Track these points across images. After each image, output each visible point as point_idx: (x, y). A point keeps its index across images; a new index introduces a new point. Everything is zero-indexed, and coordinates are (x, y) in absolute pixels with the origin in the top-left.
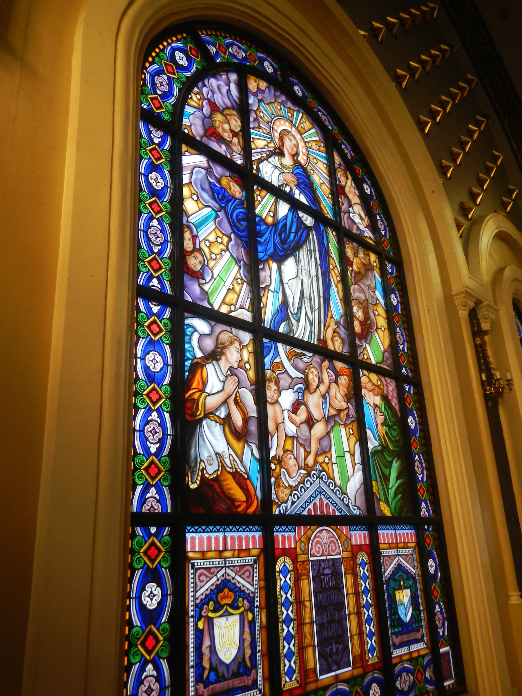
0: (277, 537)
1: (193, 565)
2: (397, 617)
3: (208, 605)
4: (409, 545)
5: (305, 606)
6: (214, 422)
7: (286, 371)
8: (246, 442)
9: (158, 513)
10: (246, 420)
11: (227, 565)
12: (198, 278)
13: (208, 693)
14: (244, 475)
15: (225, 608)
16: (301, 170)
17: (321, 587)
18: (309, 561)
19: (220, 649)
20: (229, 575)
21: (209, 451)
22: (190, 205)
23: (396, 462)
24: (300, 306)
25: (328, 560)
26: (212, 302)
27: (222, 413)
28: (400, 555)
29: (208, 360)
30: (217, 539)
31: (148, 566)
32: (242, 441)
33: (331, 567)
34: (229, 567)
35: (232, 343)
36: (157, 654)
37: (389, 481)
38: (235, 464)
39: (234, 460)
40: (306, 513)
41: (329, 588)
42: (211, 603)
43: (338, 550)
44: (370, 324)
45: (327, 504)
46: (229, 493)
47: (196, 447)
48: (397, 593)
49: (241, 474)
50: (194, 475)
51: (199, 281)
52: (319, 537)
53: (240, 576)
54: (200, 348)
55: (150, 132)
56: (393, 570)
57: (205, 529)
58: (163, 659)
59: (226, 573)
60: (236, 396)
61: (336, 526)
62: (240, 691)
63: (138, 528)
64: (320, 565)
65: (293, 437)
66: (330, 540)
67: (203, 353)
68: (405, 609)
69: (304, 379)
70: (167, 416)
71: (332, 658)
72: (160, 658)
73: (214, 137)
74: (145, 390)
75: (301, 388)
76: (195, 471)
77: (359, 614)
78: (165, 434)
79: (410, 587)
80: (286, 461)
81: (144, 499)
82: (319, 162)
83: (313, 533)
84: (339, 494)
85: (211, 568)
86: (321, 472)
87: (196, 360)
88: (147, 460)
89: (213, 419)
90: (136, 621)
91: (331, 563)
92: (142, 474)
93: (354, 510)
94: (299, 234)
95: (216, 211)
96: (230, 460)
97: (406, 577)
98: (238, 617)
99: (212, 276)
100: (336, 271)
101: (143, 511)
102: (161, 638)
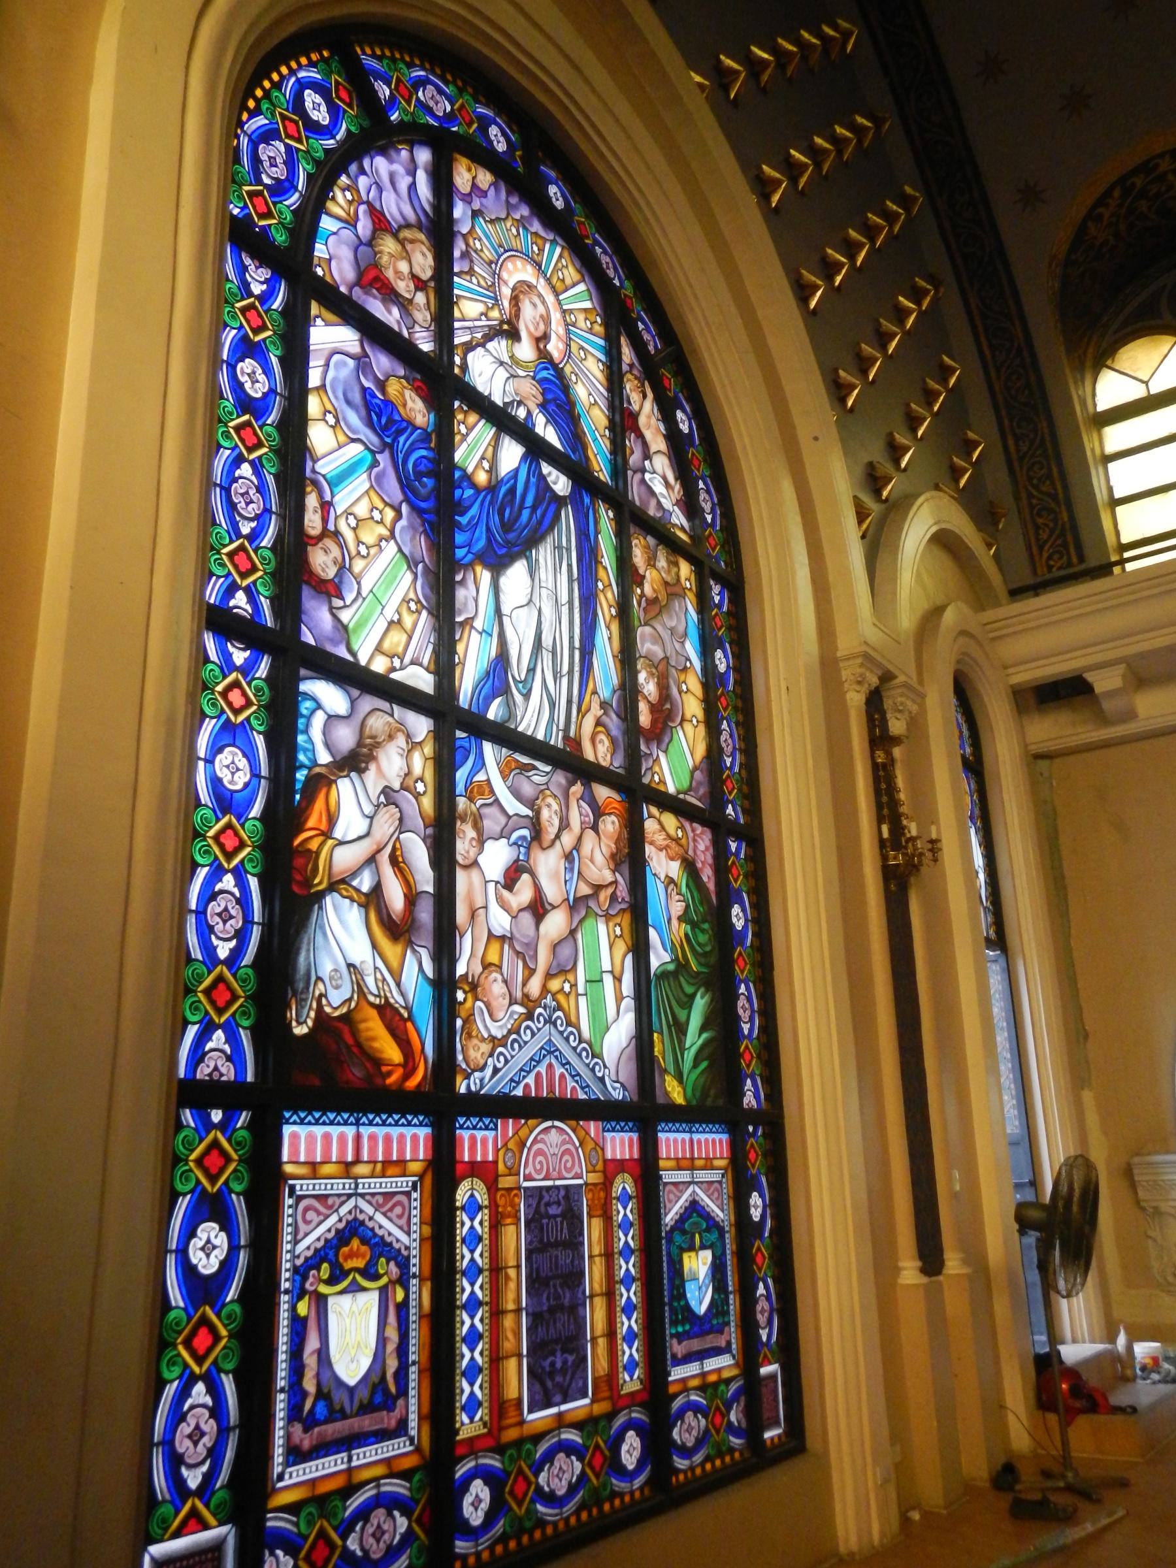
0: (462, 1138)
1: (292, 1189)
2: (682, 1303)
3: (319, 1270)
4: (717, 1163)
5: (507, 1277)
6: (347, 901)
7: (497, 801)
8: (410, 943)
9: (228, 1082)
10: (412, 898)
11: (360, 1191)
12: (329, 596)
13: (311, 1440)
14: (402, 1011)
15: (351, 1277)
16: (552, 372)
17: (541, 1240)
18: (519, 1188)
19: (337, 1357)
20: (361, 1211)
21: (335, 961)
22: (320, 436)
23: (702, 997)
24: (532, 666)
25: (557, 1188)
26: (355, 647)
27: (365, 883)
28: (697, 1183)
29: (342, 771)
30: (342, 1138)
31: (204, 1189)
32: (402, 939)
33: (562, 1202)
34: (362, 1196)
35: (391, 737)
36: (215, 1362)
37: (685, 1034)
38: (386, 988)
39: (384, 980)
40: (519, 1092)
41: (556, 1245)
42: (325, 1266)
43: (577, 1169)
44: (670, 710)
45: (562, 1076)
46: (371, 1048)
47: (308, 950)
48: (686, 1256)
49: (396, 1010)
50: (303, 1007)
51: (330, 602)
52: (543, 1141)
53: (384, 1214)
54: (327, 745)
55: (245, 269)
56: (682, 1211)
57: (321, 1117)
58: (227, 1373)
59: (356, 1207)
60: (394, 849)
61: (577, 1120)
62: (373, 1439)
63: (187, 1111)
64: (541, 1197)
65: (502, 938)
66: (563, 1148)
67: (332, 755)
68: (700, 1288)
69: (531, 819)
70: (253, 883)
71: (553, 1380)
72: (220, 1370)
73: (377, 289)
74: (211, 828)
75: (523, 838)
76: (305, 1000)
77: (610, 1295)
78: (248, 921)
79: (711, 1247)
80: (486, 986)
81: (200, 1053)
82: (590, 358)
83: (531, 1132)
84: (587, 1057)
85: (327, 1196)
86: (554, 1011)
87: (317, 770)
88: (210, 972)
89: (345, 893)
90: (176, 1296)
91: (562, 1193)
92: (200, 1001)
93: (615, 1089)
94: (539, 512)
95: (373, 453)
96: (376, 979)
97: (704, 1225)
98: (375, 1296)
99: (359, 593)
100: (609, 595)
101: (198, 1076)
102: (224, 1332)
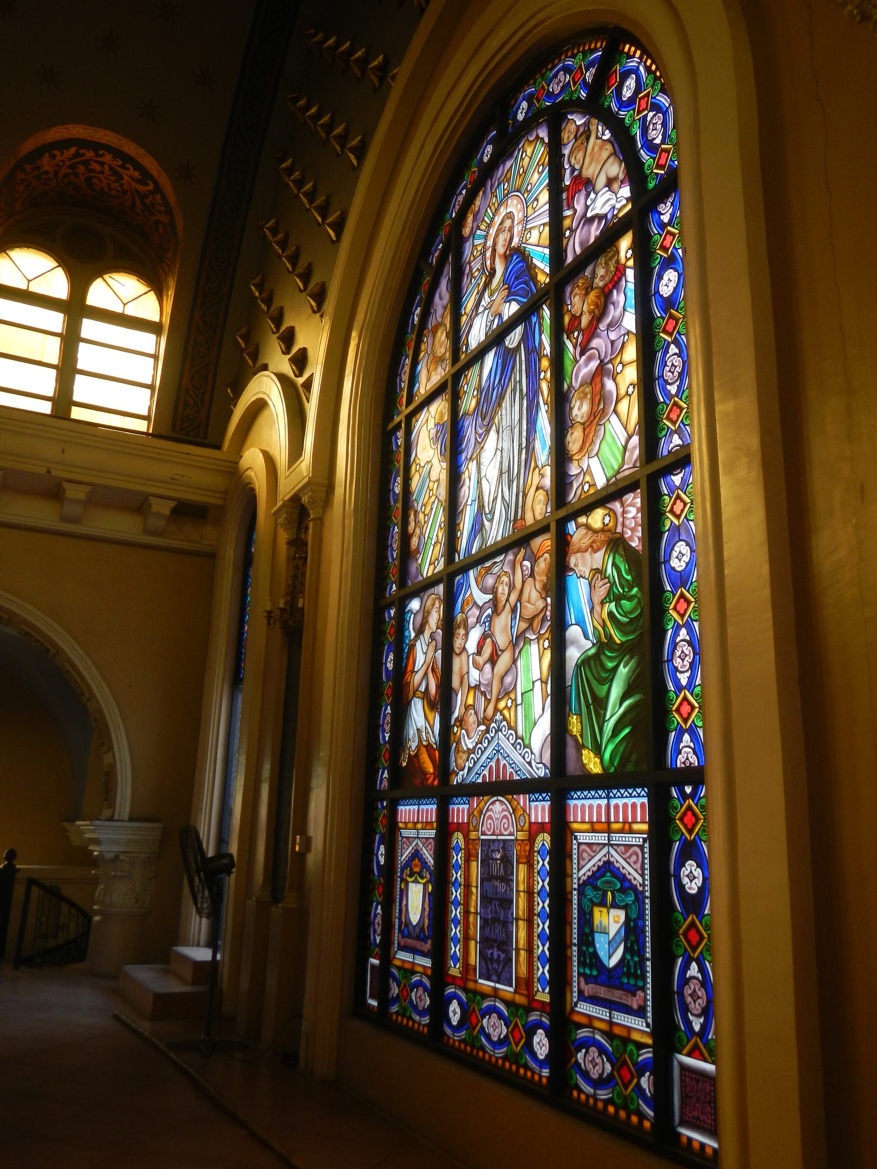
2: (591, 950)
4: (636, 827)
17: (488, 874)
23: (625, 667)
24: (496, 495)
25: (498, 840)
28: (612, 845)
33: (501, 851)
37: (606, 709)
40: (480, 780)
41: (497, 878)
43: (511, 829)
45: (504, 765)
48: (596, 910)
52: (491, 810)
56: (595, 869)
64: (489, 846)
68: (609, 942)
71: (492, 965)
79: (625, 907)
83: (486, 804)
86: (501, 722)
91: (501, 845)
93: (538, 769)
97: (619, 886)
